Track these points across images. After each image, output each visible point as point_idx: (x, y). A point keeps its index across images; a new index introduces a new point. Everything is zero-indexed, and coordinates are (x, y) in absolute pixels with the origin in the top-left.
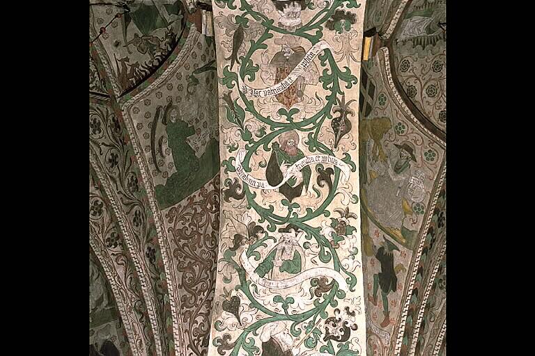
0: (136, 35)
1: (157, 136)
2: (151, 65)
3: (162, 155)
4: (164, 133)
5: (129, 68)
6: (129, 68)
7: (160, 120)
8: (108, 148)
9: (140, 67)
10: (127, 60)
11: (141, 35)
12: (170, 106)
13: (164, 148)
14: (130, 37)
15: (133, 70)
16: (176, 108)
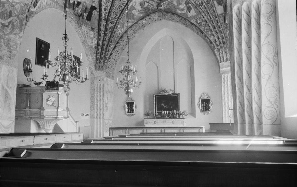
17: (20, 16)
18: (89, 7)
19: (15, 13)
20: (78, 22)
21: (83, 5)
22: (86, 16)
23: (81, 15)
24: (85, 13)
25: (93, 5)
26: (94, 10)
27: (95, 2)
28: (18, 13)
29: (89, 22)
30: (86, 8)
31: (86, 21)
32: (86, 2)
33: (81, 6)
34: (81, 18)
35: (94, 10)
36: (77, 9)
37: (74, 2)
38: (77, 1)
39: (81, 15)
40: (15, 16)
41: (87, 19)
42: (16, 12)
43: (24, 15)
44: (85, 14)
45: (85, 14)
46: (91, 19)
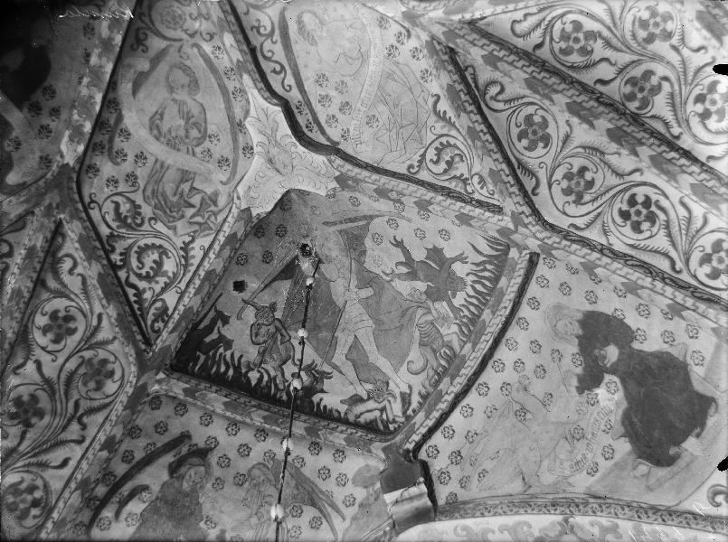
0: (273, 307)
1: (143, 478)
2: (244, 371)
3: (117, 514)
4: (156, 488)
5: (214, 336)
6: (214, 336)
7: (169, 458)
8: (37, 378)
9: (228, 353)
10: (226, 321)
11: (278, 315)
12: (202, 454)
13: (136, 507)
14: (265, 299)
15: (215, 344)
16: (207, 466)
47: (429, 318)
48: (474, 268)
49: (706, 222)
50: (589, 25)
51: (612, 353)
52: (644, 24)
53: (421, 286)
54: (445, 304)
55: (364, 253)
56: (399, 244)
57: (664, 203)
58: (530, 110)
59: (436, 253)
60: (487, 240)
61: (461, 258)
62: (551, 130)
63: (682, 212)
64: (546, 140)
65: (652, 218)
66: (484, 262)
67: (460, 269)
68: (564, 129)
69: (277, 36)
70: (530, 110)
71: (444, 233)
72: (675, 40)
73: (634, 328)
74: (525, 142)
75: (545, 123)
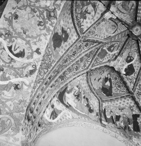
17: (15, 114)
18: (131, 117)
19: (5, 110)
20: (124, 135)
21: (123, 117)
22: (133, 127)
23: (125, 128)
24: (129, 125)
25: (134, 113)
26: (138, 118)
27: (134, 110)
28: (10, 110)
29: (139, 133)
30: (128, 119)
31: (135, 132)
32: (125, 114)
33: (121, 119)
34: (127, 131)
35: (138, 118)
36: (118, 123)
37: (112, 116)
38: (115, 116)
39: (126, 128)
40: (7, 113)
41: (135, 130)
42: (7, 109)
43: (21, 113)
44: (130, 126)
45: (130, 126)
46: (139, 129)
47: (80, 9)
48: (81, 22)
49: (69, 61)
50: (89, 58)
51: (64, 36)
52: (85, 64)
53: (84, 11)
54: (80, 13)
55: (92, 6)
56: (90, 13)
57: (73, 57)
58: (88, 46)
59: (85, 18)
60: (83, 29)
61: (83, 22)
62: (85, 47)
63: (72, 59)
64: (85, 46)
65: (73, 55)
66: (80, 25)
67: (82, 20)
68: (85, 49)
69: (117, 23)
70: (88, 46)
71: (87, 22)
72: (83, 67)
73: (65, 43)
74: (87, 43)
75: (86, 47)
